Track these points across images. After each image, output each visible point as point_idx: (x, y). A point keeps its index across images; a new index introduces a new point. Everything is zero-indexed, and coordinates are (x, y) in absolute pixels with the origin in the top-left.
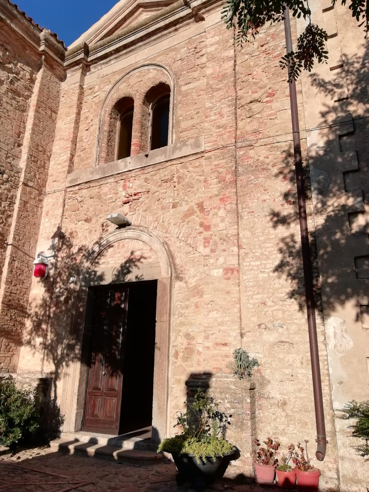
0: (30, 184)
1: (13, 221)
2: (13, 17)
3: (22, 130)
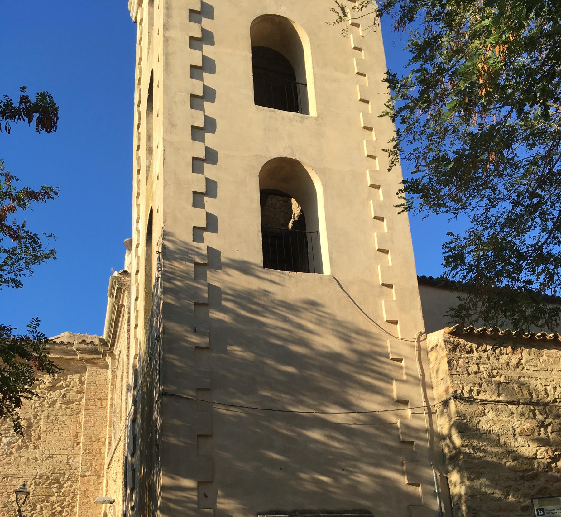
3: (79, 430)
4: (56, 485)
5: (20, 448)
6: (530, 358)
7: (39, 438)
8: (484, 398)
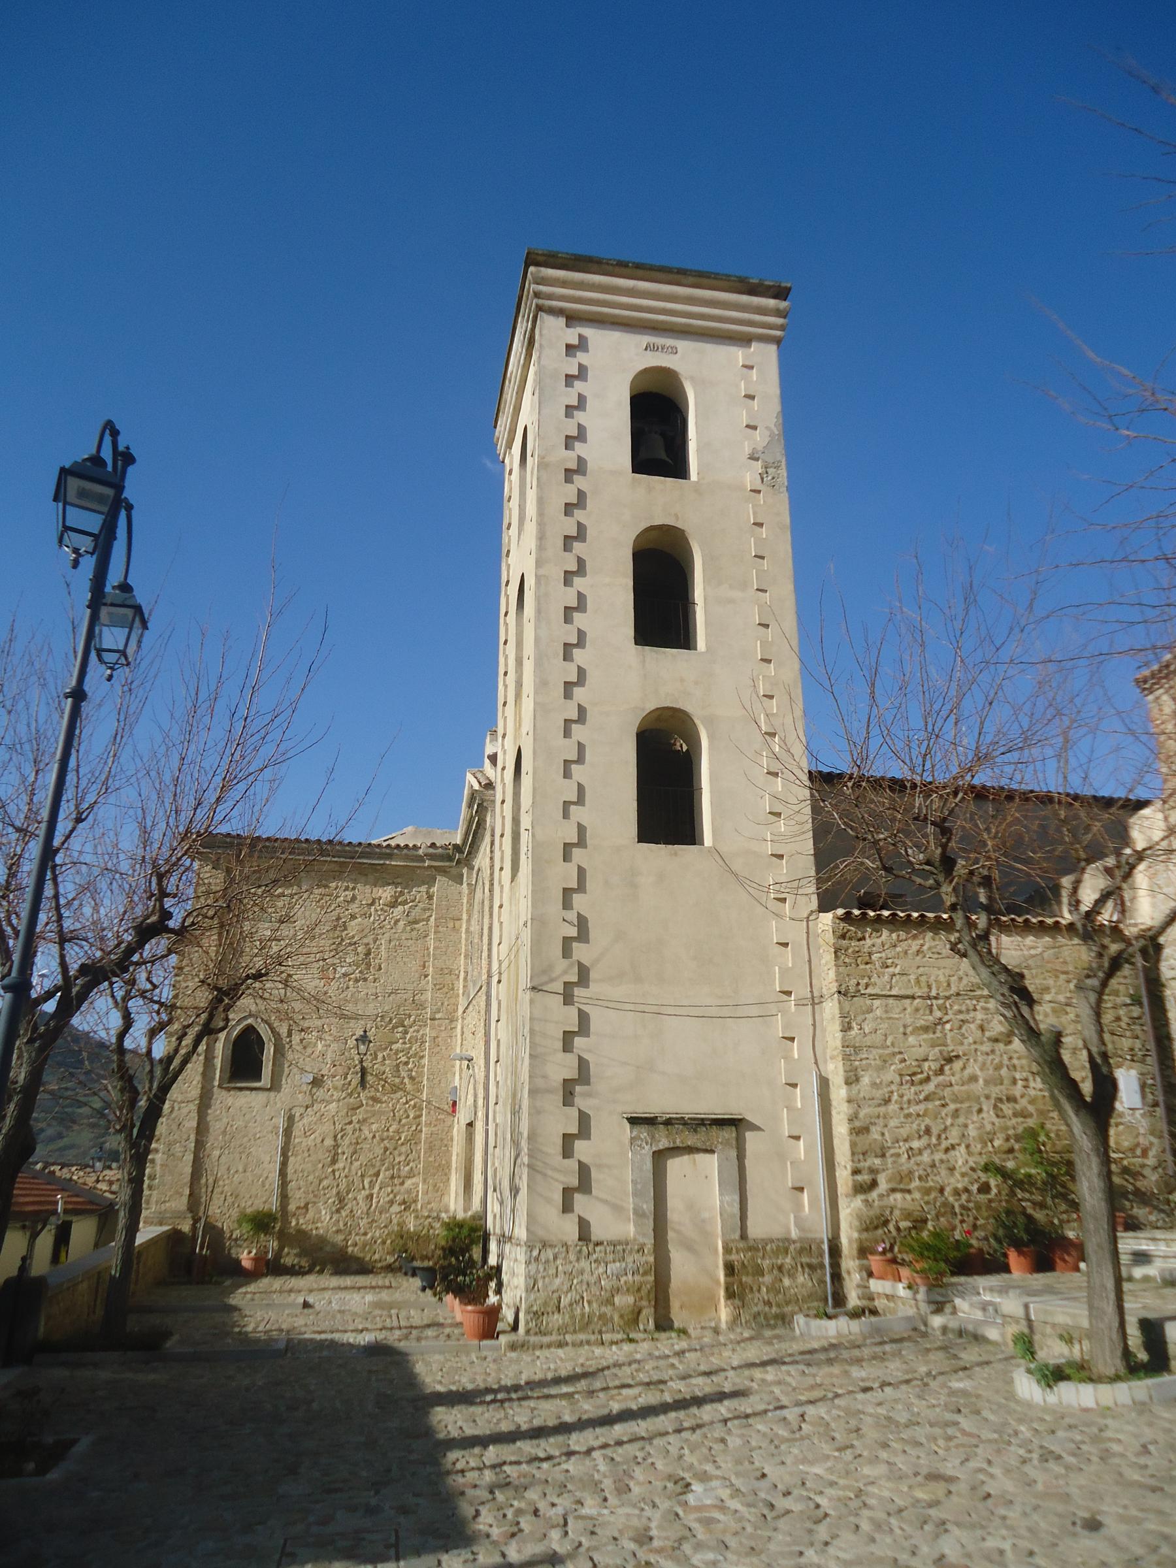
0: (438, 1016)
1: (426, 1061)
2: (390, 856)
4: (400, 1029)
5: (357, 981)
6: (933, 944)
7: (380, 969)
8: (873, 992)
